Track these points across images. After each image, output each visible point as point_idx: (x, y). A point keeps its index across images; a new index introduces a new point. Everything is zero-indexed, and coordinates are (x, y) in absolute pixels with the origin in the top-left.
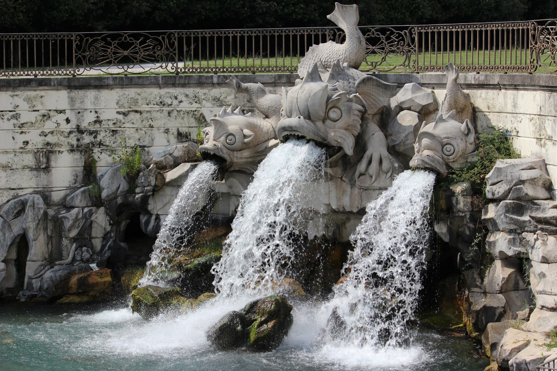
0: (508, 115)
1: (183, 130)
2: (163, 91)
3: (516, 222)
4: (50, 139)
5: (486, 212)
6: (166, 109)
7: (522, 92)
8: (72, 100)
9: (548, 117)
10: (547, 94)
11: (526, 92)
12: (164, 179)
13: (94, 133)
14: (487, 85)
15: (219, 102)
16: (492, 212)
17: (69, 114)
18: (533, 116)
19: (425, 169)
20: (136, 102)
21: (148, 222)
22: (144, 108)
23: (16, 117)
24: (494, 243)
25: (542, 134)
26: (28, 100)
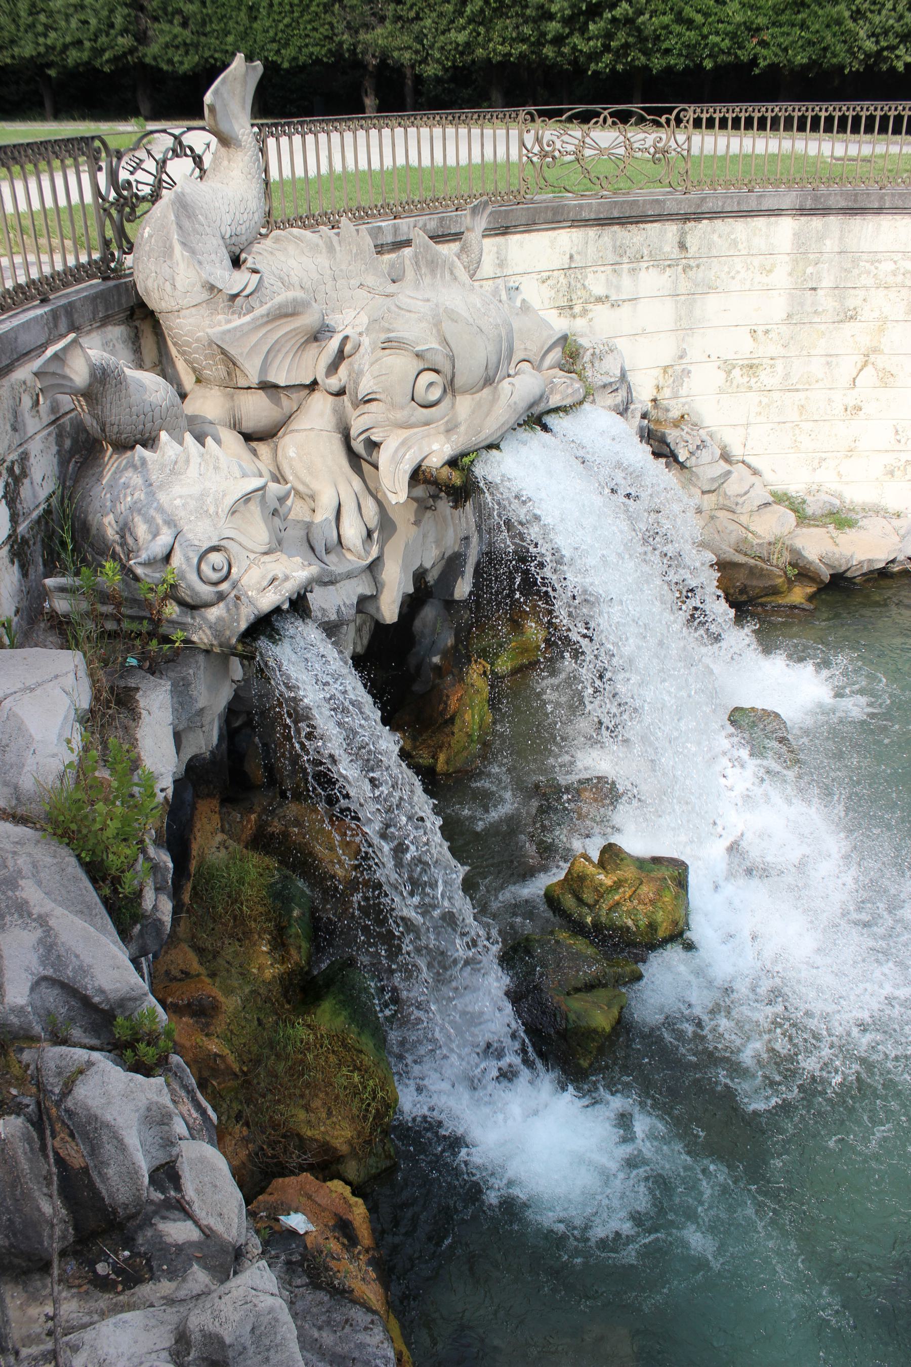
0: (484, 282)
7: (518, 236)
9: (594, 269)
10: (592, 232)
11: (526, 235)
14: (443, 236)
18: (548, 274)
25: (574, 297)
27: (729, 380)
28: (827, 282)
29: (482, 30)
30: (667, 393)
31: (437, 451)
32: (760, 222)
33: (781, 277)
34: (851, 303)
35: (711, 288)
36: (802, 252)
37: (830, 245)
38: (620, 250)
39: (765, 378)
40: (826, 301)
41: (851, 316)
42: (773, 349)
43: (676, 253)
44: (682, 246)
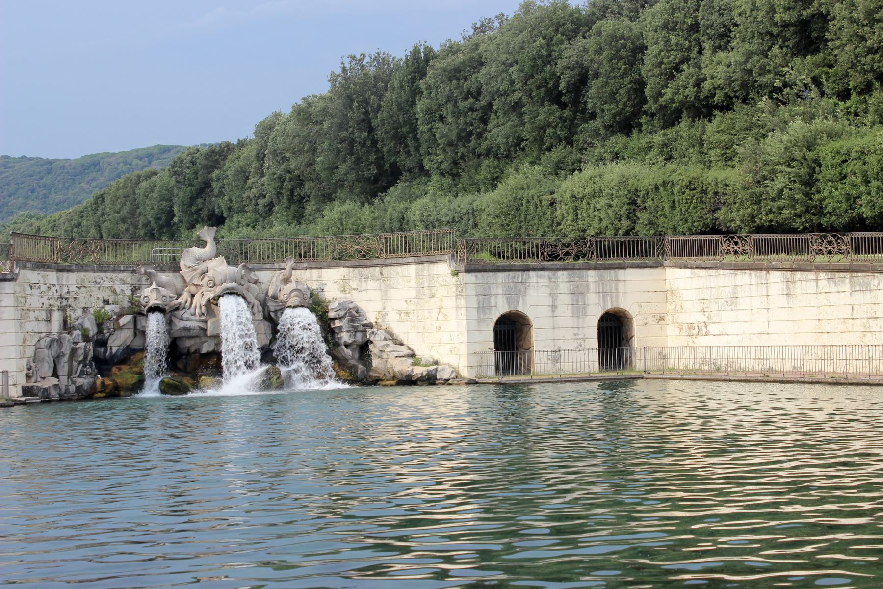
1: (106, 298)
2: (96, 274)
3: (353, 327)
4: (51, 302)
5: (334, 324)
6: (98, 285)
8: (58, 278)
10: (351, 270)
12: (119, 324)
13: (67, 299)
15: (123, 282)
16: (337, 323)
17: (57, 287)
19: (302, 306)
20: (84, 280)
21: (105, 351)
22: (87, 284)
23: (39, 287)
24: (341, 338)
26: (43, 277)
27: (401, 317)
28: (426, 285)
29: (755, 208)
30: (380, 320)
31: (212, 296)
32: (405, 266)
33: (413, 283)
34: (433, 291)
35: (392, 287)
36: (418, 276)
37: (426, 273)
38: (361, 275)
39: (412, 317)
40: (426, 291)
41: (433, 296)
42: (413, 307)
43: (379, 276)
44: (382, 274)
